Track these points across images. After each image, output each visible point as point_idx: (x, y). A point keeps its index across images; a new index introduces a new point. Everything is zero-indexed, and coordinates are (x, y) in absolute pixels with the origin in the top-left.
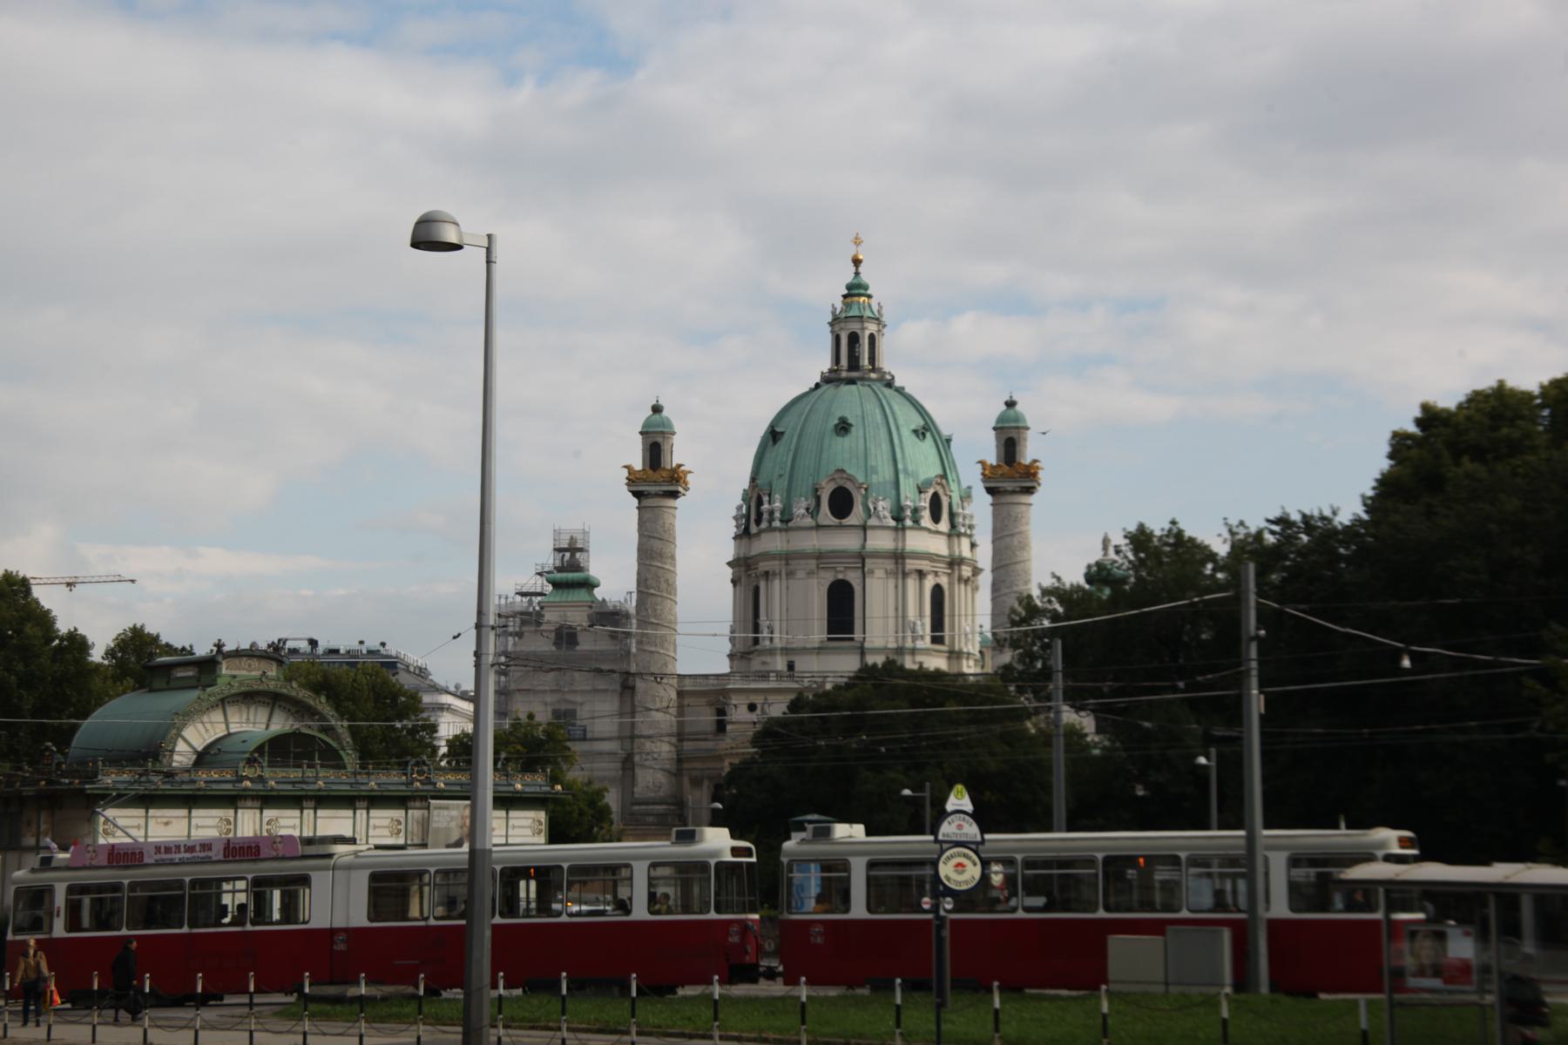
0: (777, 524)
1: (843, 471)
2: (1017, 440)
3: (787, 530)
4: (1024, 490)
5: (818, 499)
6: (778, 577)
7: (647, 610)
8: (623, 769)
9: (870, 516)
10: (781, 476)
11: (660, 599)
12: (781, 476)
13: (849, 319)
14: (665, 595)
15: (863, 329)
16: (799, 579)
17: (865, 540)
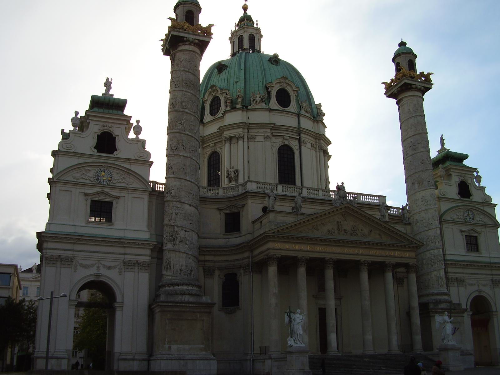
0: (239, 106)
1: (286, 78)
2: (414, 64)
3: (247, 110)
4: (424, 90)
5: (269, 93)
6: (242, 139)
7: (184, 124)
8: (151, 257)
9: (301, 110)
10: (237, 82)
11: (193, 118)
12: (236, 82)
13: (250, 27)
14: (196, 116)
15: (257, 34)
16: (257, 142)
17: (299, 123)
